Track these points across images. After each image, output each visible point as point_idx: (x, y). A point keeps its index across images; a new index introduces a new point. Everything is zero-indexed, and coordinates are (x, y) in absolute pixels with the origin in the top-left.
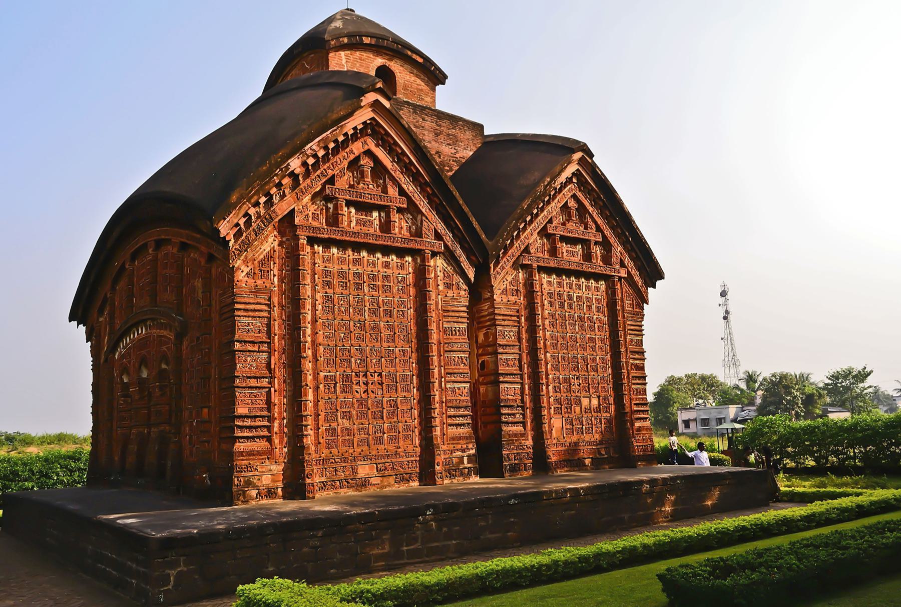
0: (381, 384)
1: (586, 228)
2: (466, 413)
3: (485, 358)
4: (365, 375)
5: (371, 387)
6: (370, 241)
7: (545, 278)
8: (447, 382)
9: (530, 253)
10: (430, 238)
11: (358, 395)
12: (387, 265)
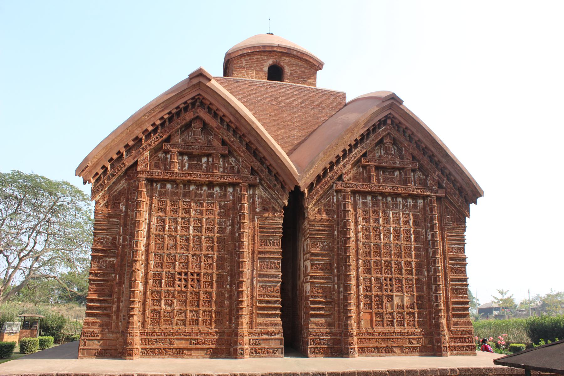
0: (199, 281)
1: (402, 158)
2: (276, 305)
3: (305, 263)
4: (186, 274)
5: (190, 282)
6: (195, 179)
7: (360, 201)
8: (257, 281)
9: (343, 181)
10: (246, 173)
11: (179, 289)
12: (211, 195)
